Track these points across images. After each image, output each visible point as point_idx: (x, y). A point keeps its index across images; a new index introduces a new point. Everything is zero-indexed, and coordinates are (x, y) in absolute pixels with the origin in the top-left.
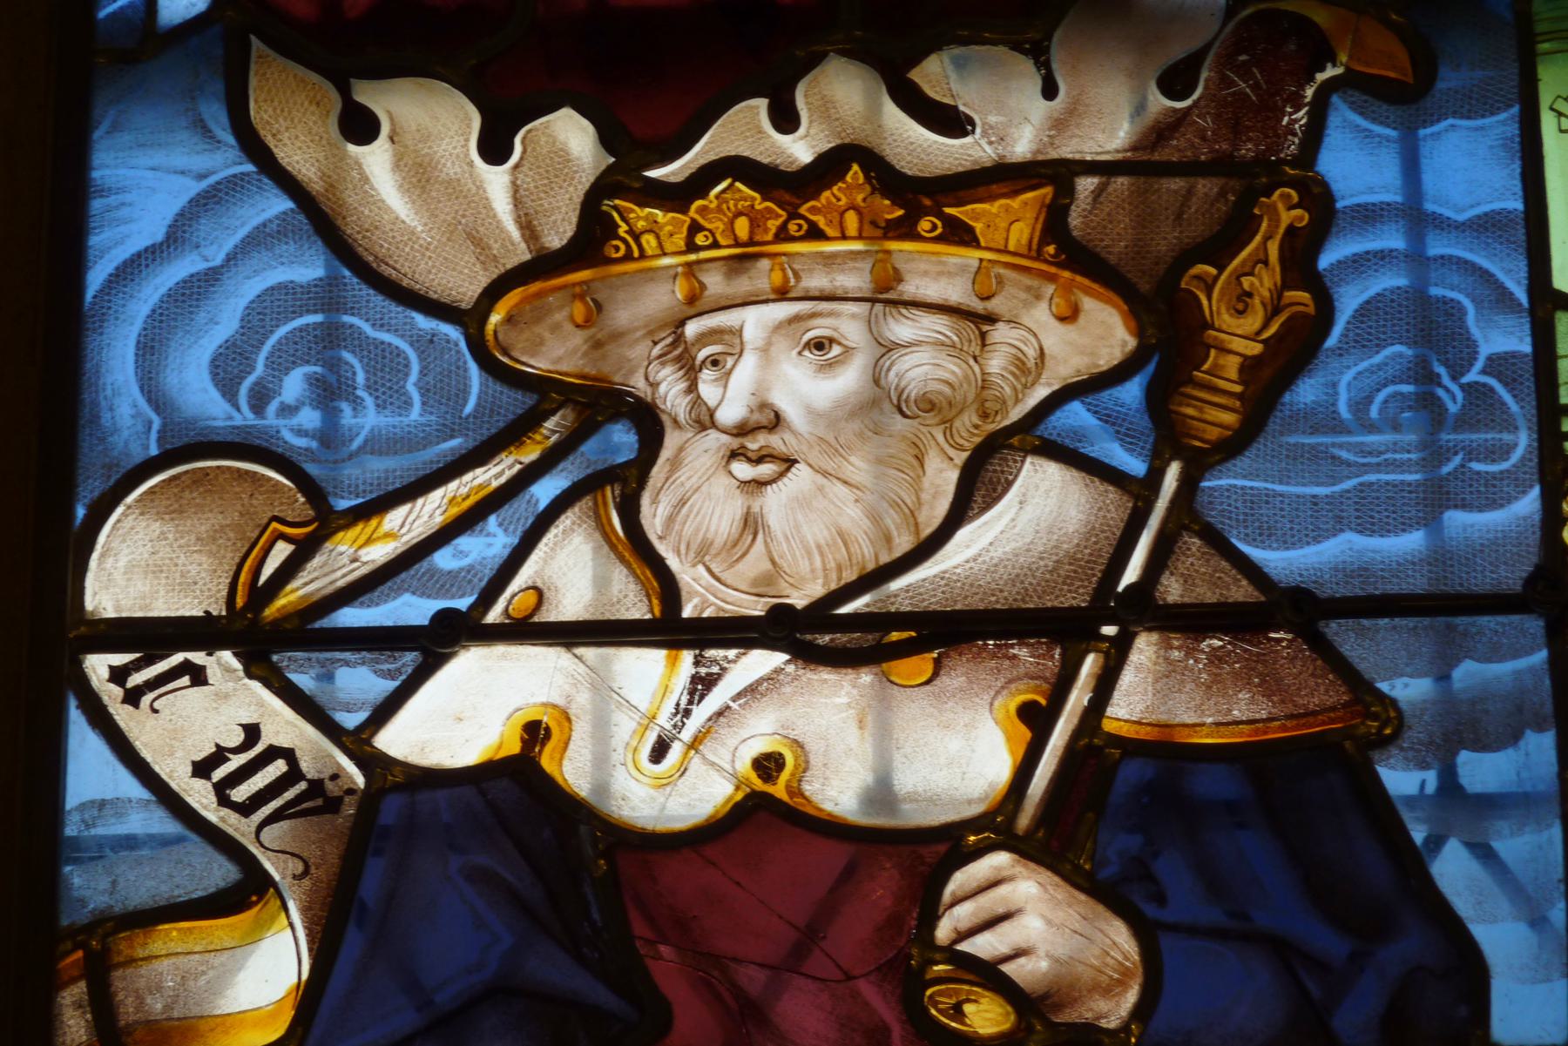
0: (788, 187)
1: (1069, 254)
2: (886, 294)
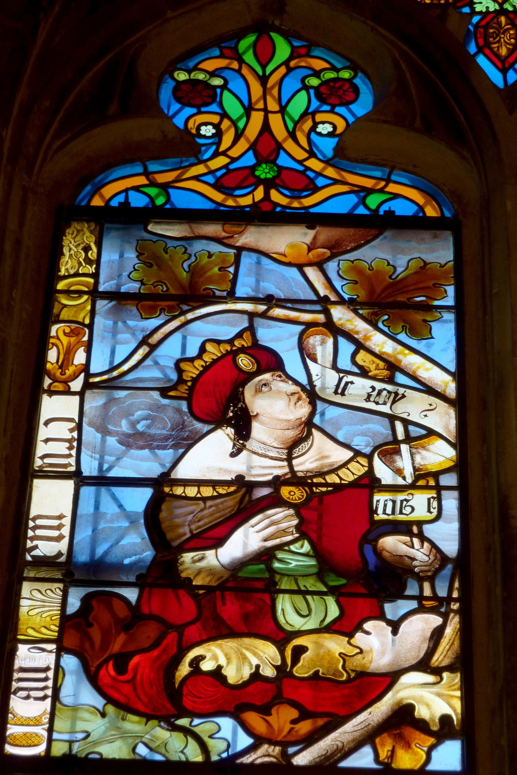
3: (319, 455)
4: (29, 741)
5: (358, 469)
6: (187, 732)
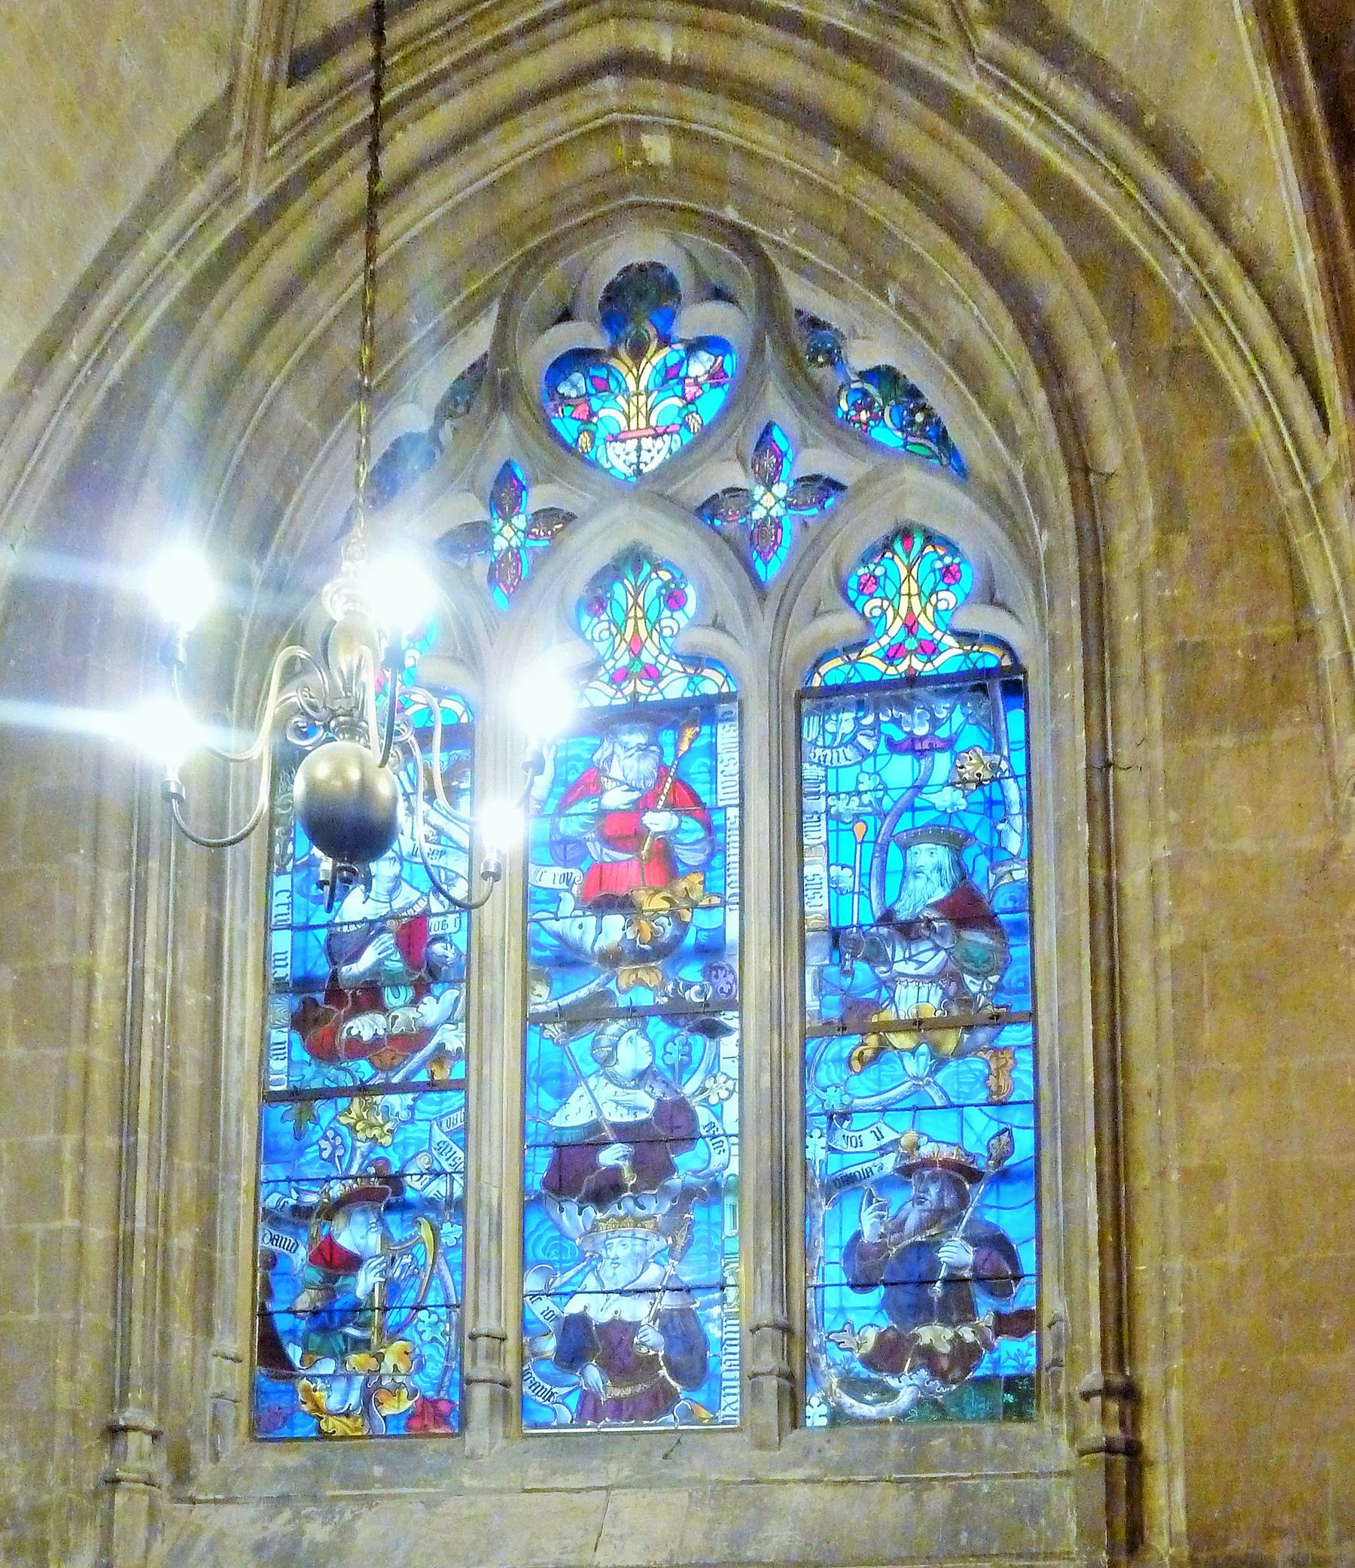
0: (621, 1219)
1: (658, 1231)
2: (633, 1237)
3: (406, 895)
4: (279, 1083)
5: (422, 904)
6: (344, 1069)
